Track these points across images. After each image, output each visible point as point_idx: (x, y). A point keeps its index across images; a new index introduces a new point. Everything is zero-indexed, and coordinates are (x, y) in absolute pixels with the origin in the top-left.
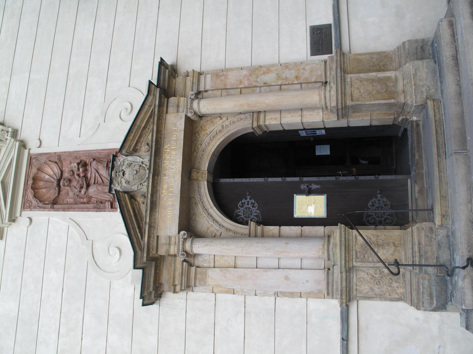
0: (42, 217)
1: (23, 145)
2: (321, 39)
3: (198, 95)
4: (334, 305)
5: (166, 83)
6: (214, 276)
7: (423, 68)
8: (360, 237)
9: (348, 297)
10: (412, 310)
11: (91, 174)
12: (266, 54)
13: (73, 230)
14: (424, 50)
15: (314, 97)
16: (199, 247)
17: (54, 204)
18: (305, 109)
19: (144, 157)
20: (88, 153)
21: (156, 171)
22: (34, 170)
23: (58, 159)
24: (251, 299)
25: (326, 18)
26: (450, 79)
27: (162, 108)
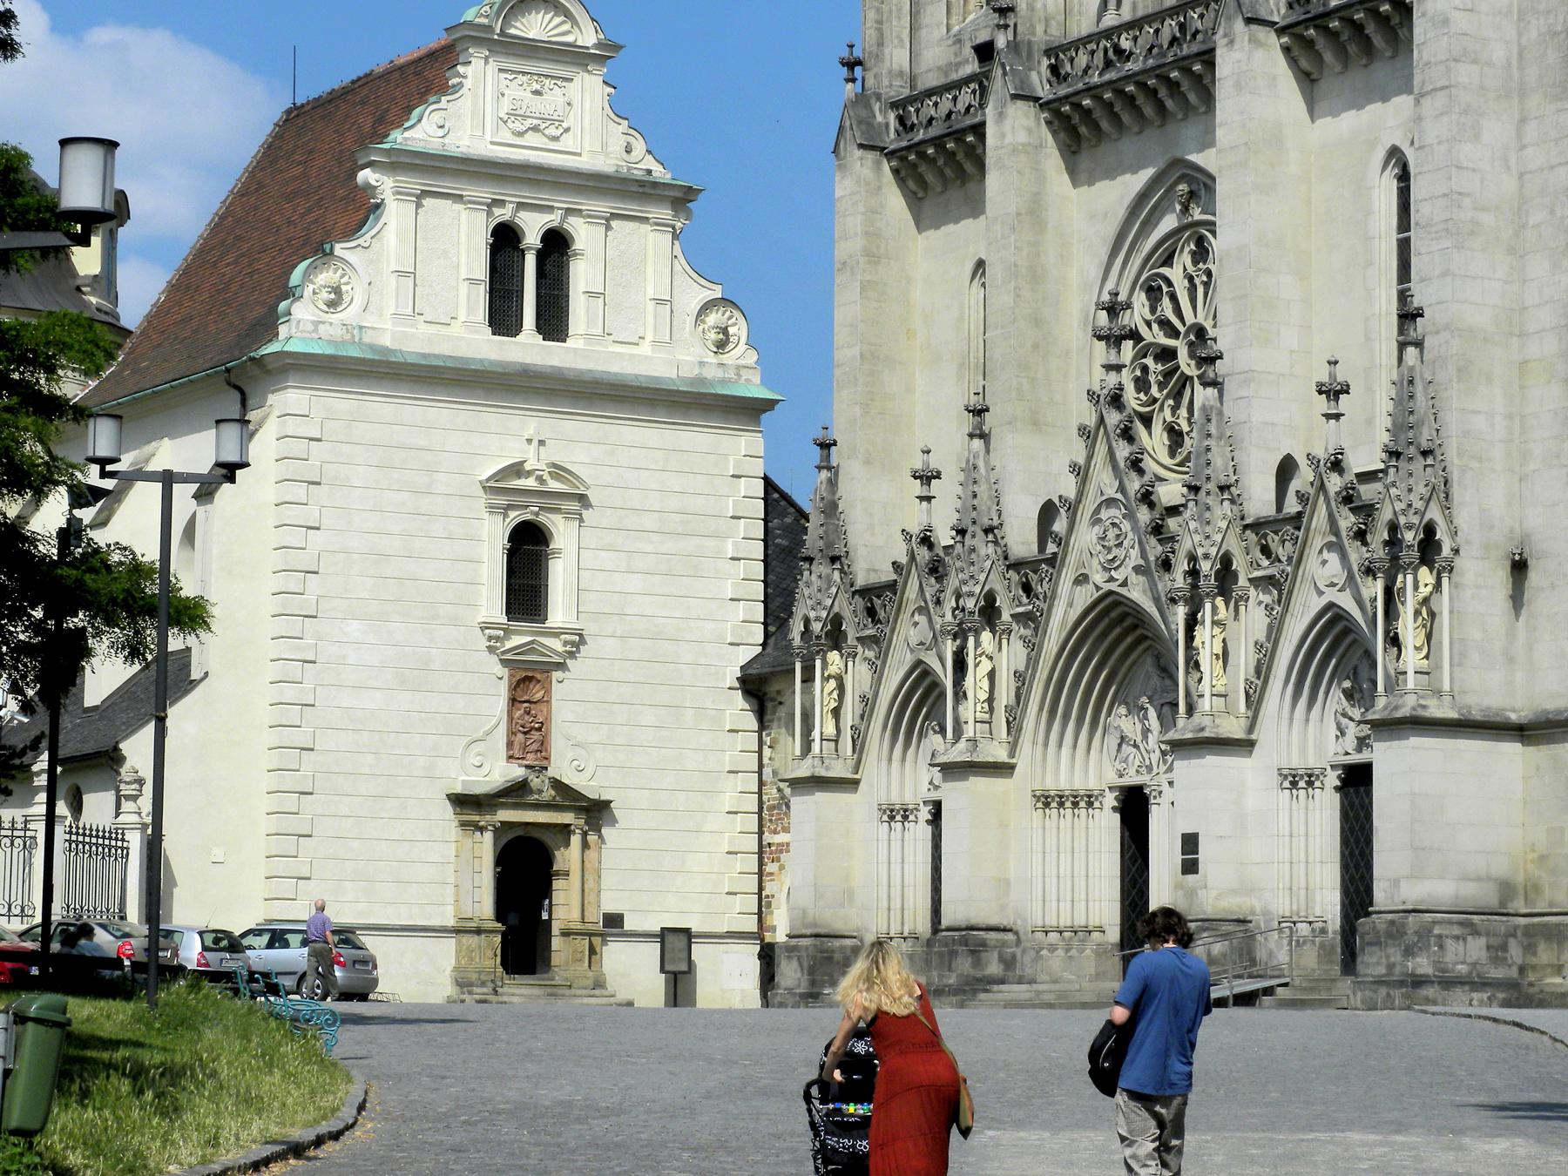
0: (503, 689)
1: (561, 666)
2: (614, 921)
3: (585, 834)
4: (451, 923)
5: (596, 812)
6: (468, 842)
7: (590, 983)
8: (498, 939)
9: (457, 931)
10: (450, 968)
11: (535, 735)
12: (607, 880)
13: (494, 721)
14: (599, 984)
15: (576, 914)
16: (488, 837)
17: (513, 701)
18: (564, 906)
19: (549, 794)
20: (548, 731)
21: (538, 806)
22: (538, 676)
23: (546, 701)
24: (452, 868)
25: (628, 925)
26: (584, 992)
27: (579, 810)
